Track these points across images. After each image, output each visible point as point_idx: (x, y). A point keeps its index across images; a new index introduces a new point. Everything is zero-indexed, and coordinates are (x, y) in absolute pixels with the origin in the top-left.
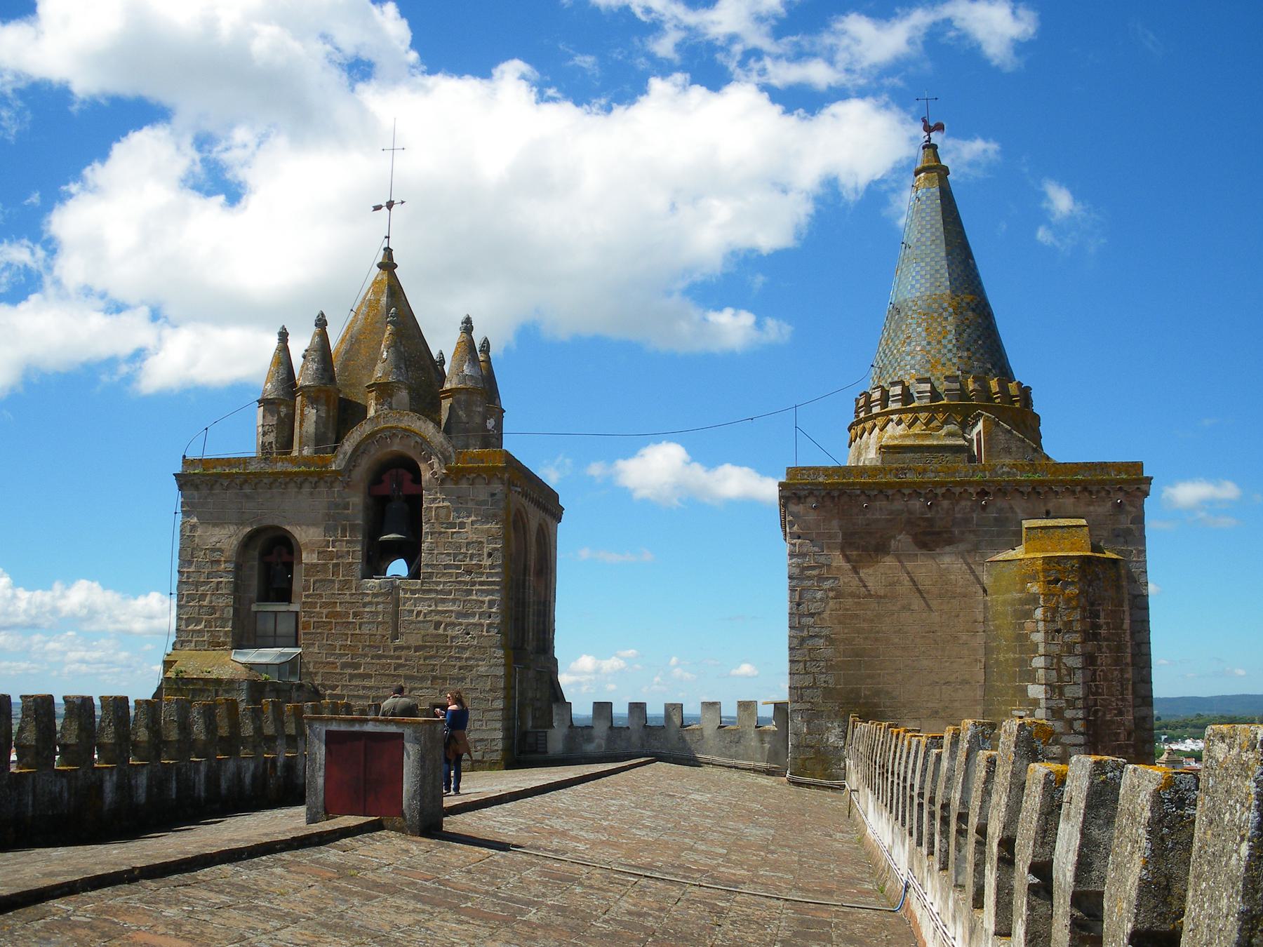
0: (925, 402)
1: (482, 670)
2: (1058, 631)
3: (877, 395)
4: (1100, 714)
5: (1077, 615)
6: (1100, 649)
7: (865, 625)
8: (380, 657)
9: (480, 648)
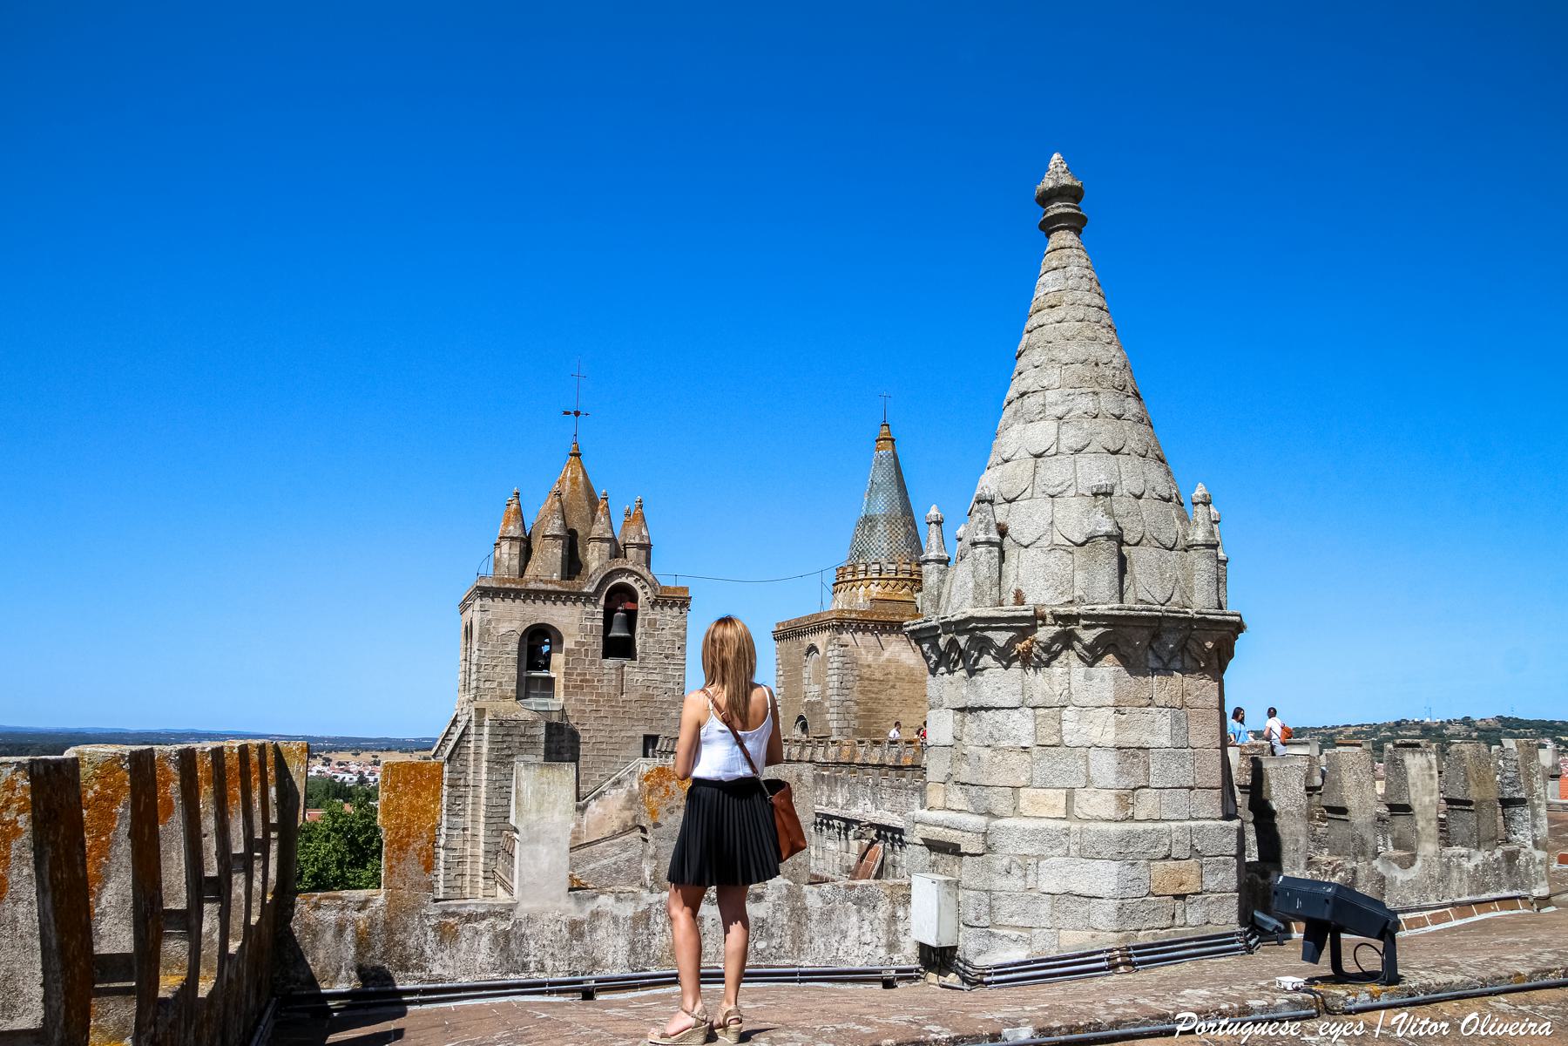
1: (674, 714)
7: (873, 695)
9: (673, 702)
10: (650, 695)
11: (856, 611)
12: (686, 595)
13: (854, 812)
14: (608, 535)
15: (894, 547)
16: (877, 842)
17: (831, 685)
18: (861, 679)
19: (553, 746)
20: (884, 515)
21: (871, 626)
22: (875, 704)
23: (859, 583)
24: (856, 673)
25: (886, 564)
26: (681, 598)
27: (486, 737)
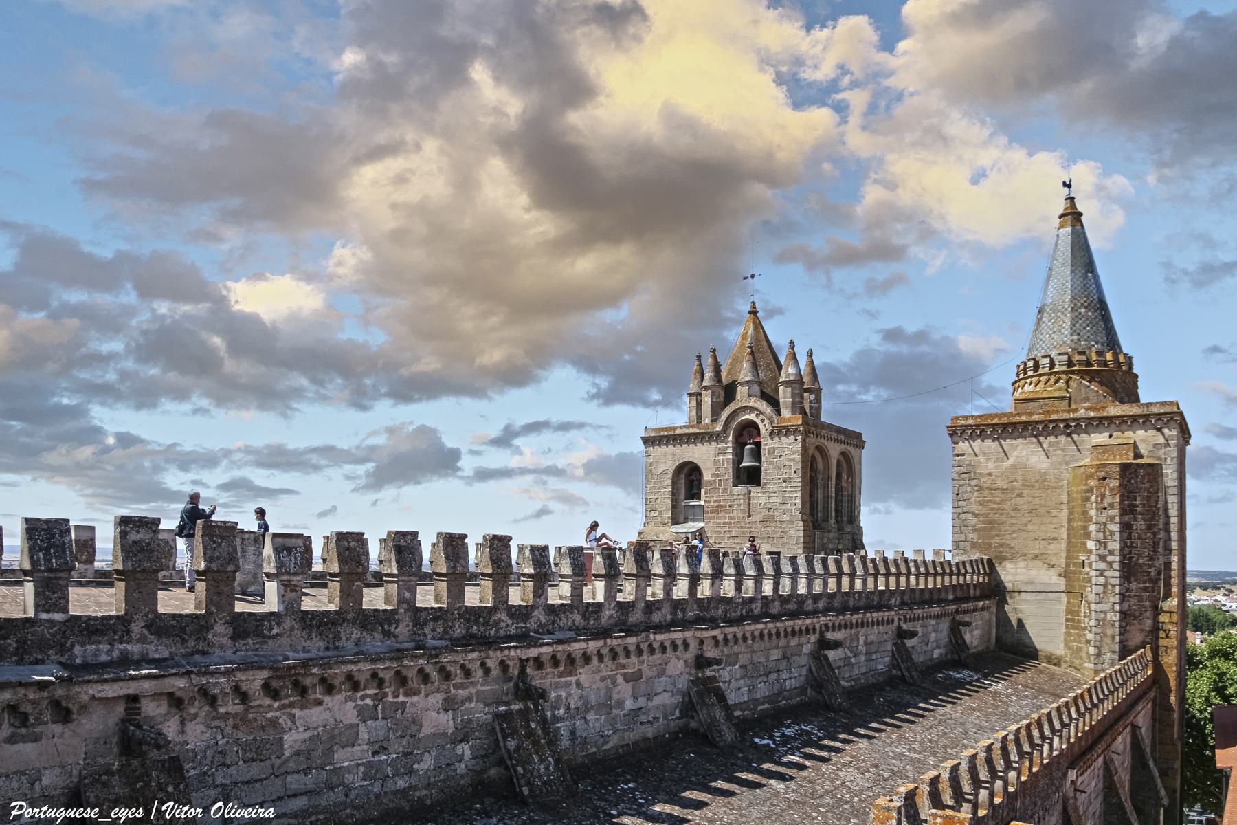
0: (1046, 370)
2: (1105, 509)
3: (1031, 364)
4: (1134, 559)
5: (1118, 499)
6: (1135, 520)
7: (995, 506)
11: (972, 416)
18: (980, 488)
22: (997, 515)
24: (974, 483)
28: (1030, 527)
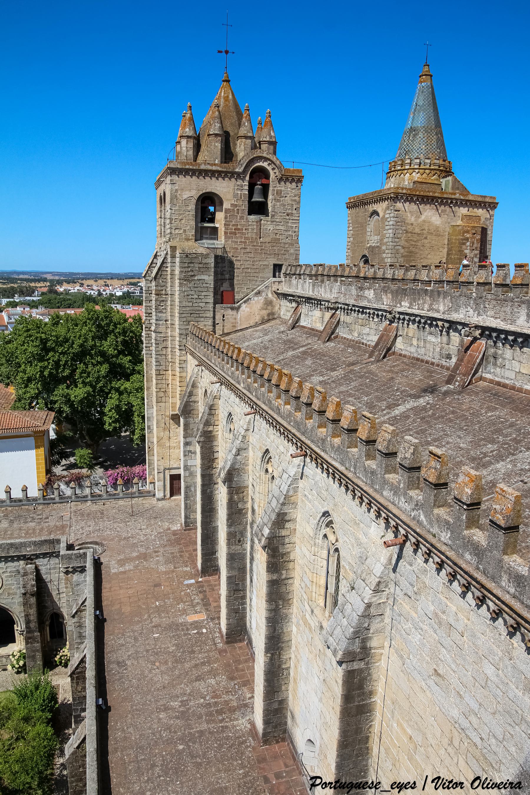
0: (428, 167)
1: (292, 251)
7: (414, 243)
8: (254, 246)
10: (278, 239)
11: (406, 188)
12: (300, 175)
13: (455, 317)
14: (250, 134)
15: (429, 148)
16: (479, 339)
17: (387, 235)
18: (407, 232)
19: (219, 270)
20: (424, 127)
21: (415, 198)
23: (406, 171)
24: (404, 228)
25: (423, 160)
26: (297, 176)
27: (178, 264)
28: (429, 256)
